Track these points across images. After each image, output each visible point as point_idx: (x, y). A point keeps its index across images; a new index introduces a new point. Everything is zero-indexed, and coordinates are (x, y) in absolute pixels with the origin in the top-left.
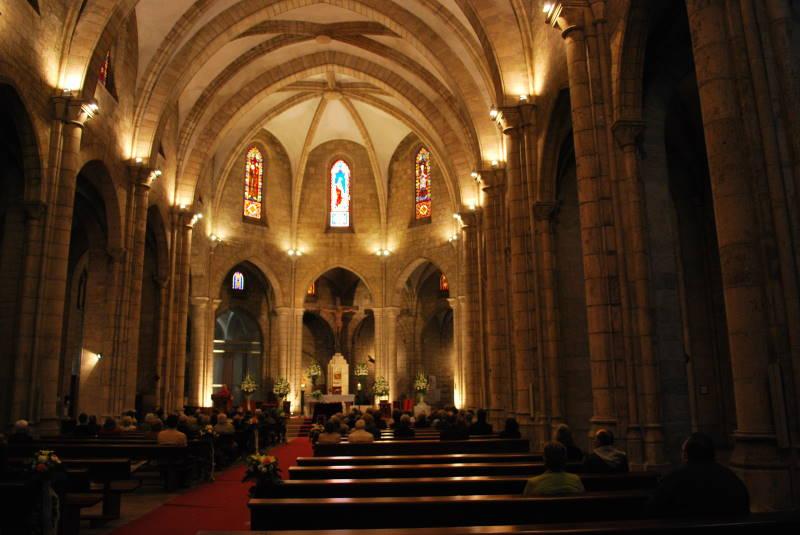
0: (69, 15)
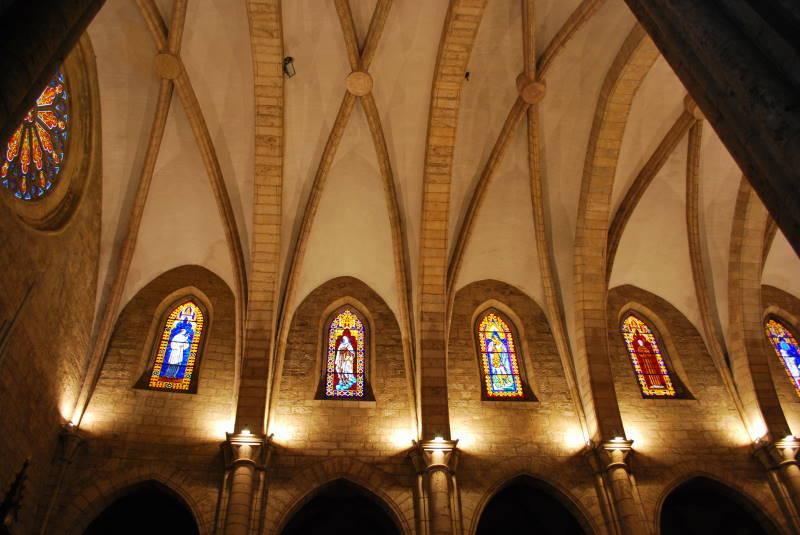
0: (722, 375)
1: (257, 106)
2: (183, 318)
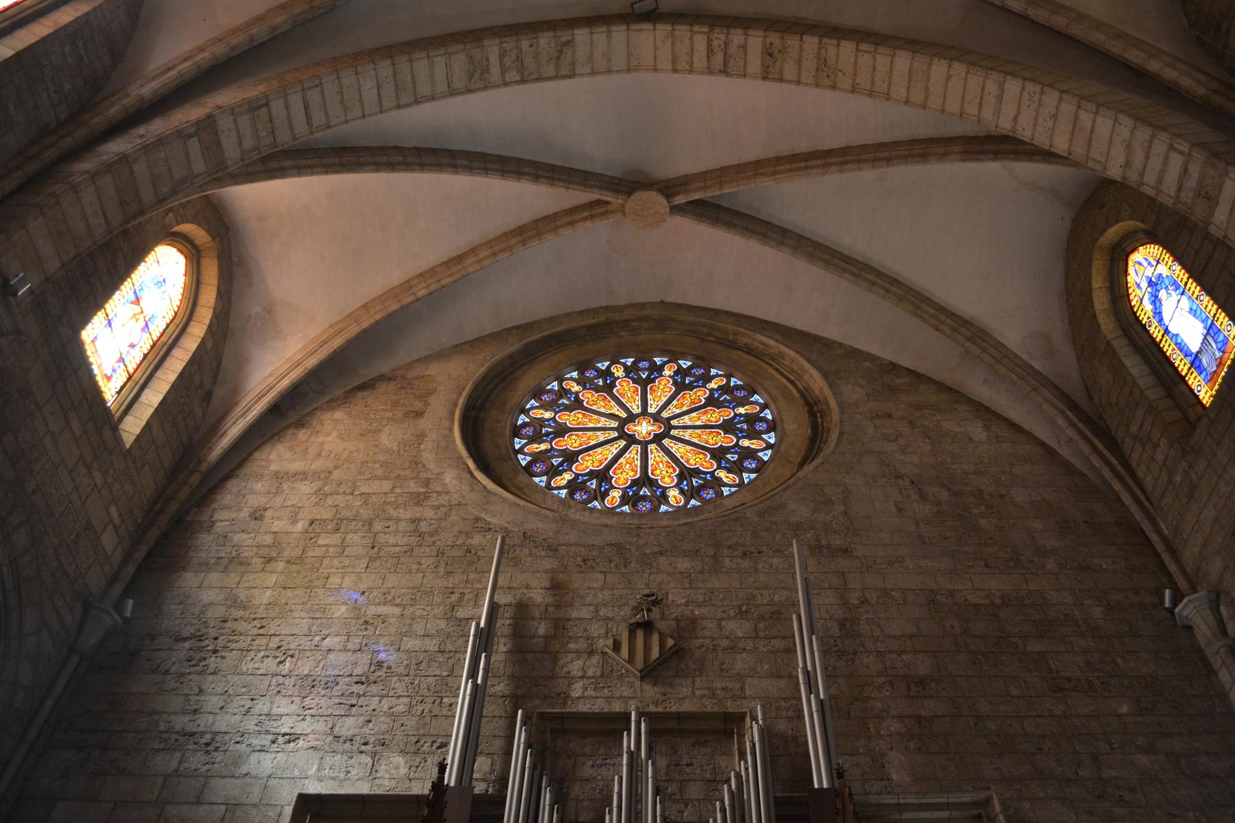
1: (710, 72)
2: (1144, 285)
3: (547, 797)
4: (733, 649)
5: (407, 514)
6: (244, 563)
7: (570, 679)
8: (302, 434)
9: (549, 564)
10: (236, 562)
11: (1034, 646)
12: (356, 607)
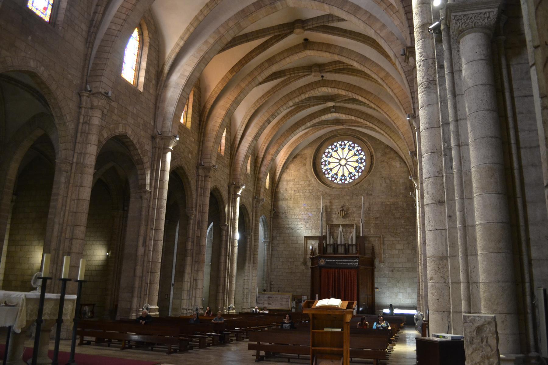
3: (331, 237)
4: (354, 213)
5: (307, 188)
6: (287, 199)
7: (333, 218)
8: (288, 171)
9: (329, 198)
10: (286, 199)
11: (394, 212)
12: (304, 207)
